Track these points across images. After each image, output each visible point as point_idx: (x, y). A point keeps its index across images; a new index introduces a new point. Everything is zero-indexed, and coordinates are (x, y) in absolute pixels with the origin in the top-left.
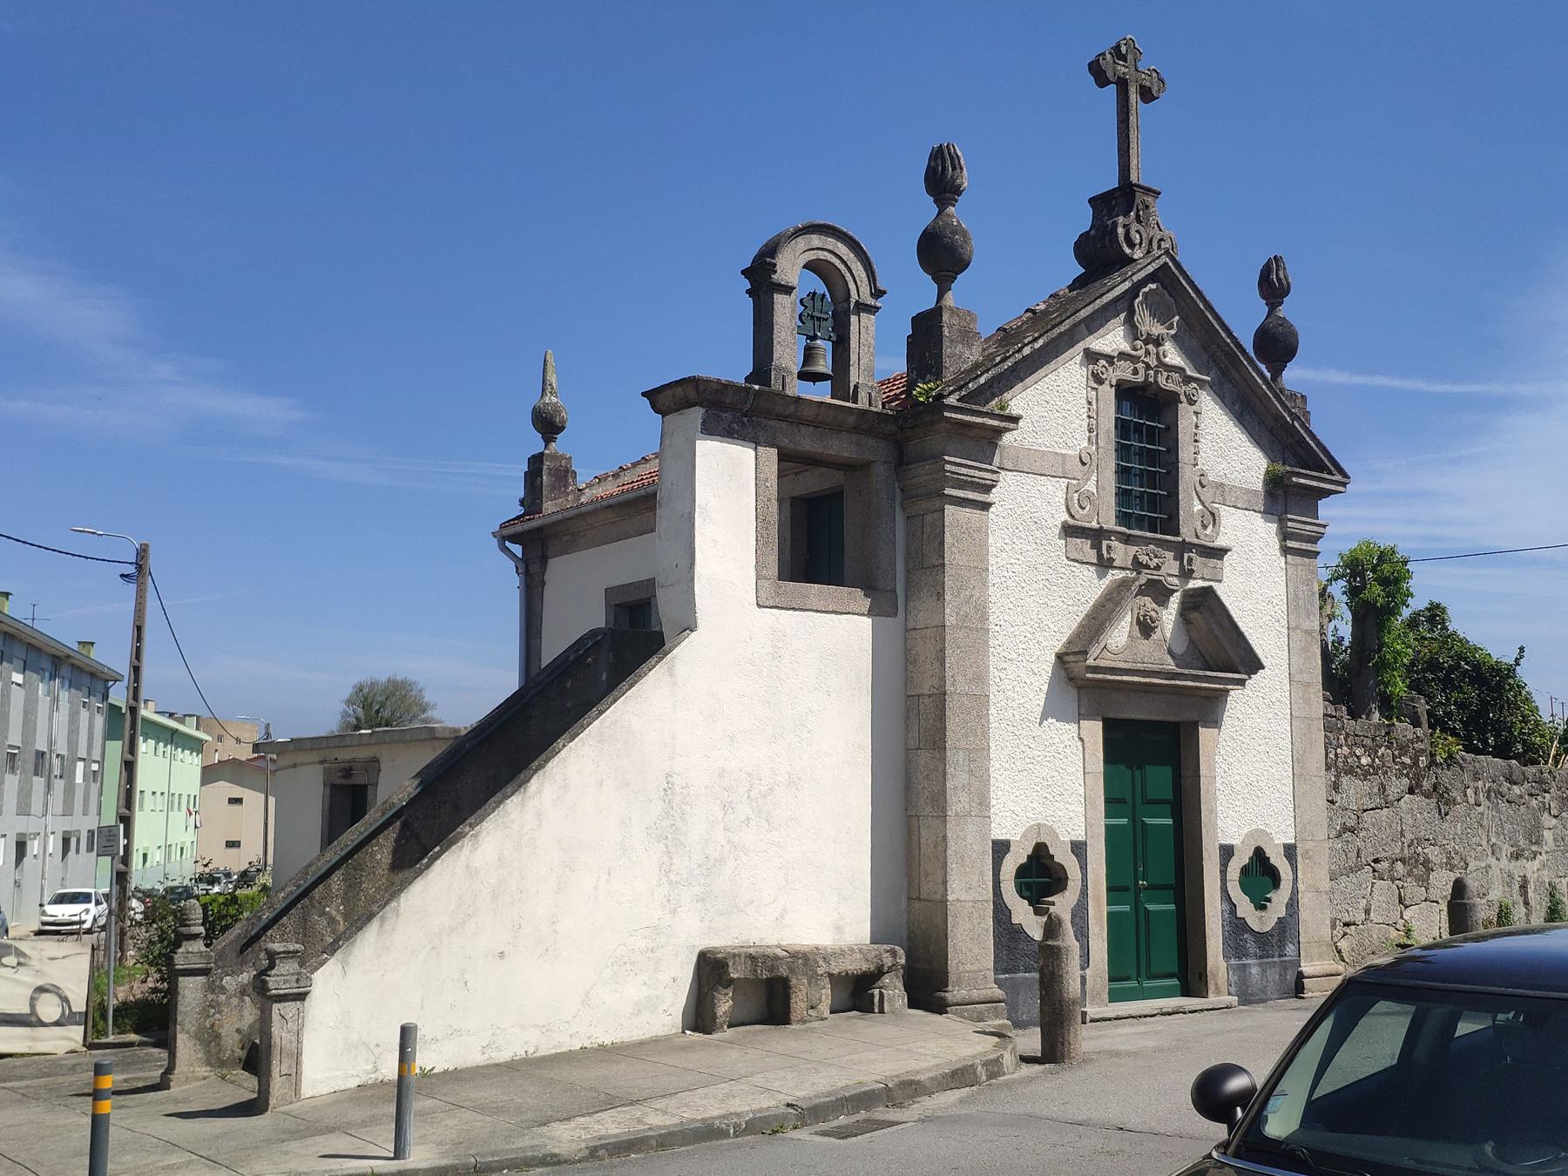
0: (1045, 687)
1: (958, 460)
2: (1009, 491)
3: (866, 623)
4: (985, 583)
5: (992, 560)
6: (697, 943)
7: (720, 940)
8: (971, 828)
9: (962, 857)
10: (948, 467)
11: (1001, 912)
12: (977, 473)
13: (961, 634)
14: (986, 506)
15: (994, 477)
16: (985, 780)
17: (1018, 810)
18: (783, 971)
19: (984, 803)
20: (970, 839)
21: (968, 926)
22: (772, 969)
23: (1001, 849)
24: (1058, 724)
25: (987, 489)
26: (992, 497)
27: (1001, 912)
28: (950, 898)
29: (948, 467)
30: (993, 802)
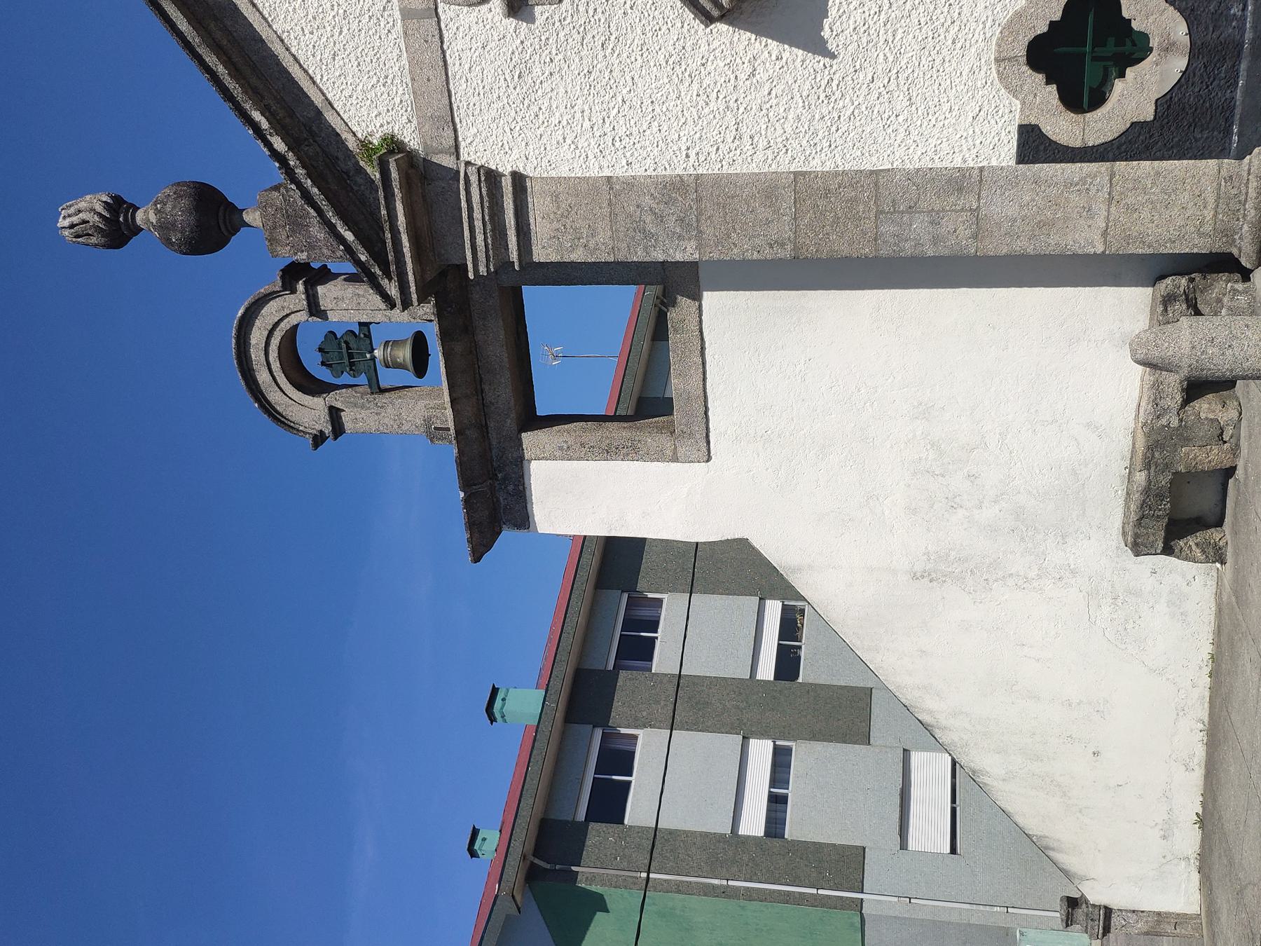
0: (773, 44)
1: (464, 204)
2: (487, 143)
3: (710, 299)
4: (630, 185)
5: (594, 172)
6: (1114, 544)
7: (1109, 507)
8: (1000, 207)
9: (1041, 225)
10: (482, 270)
11: (1135, 144)
12: (477, 214)
13: (708, 231)
14: (519, 180)
15: (474, 179)
16: (924, 179)
17: (971, 109)
18: (1164, 480)
19: (960, 182)
20: (1012, 210)
21: (1145, 214)
22: (1160, 497)
23: (1034, 145)
24: (833, 12)
25: (491, 178)
26: (506, 168)
27: (1135, 144)
28: (1100, 249)
29: (482, 270)
30: (958, 162)
